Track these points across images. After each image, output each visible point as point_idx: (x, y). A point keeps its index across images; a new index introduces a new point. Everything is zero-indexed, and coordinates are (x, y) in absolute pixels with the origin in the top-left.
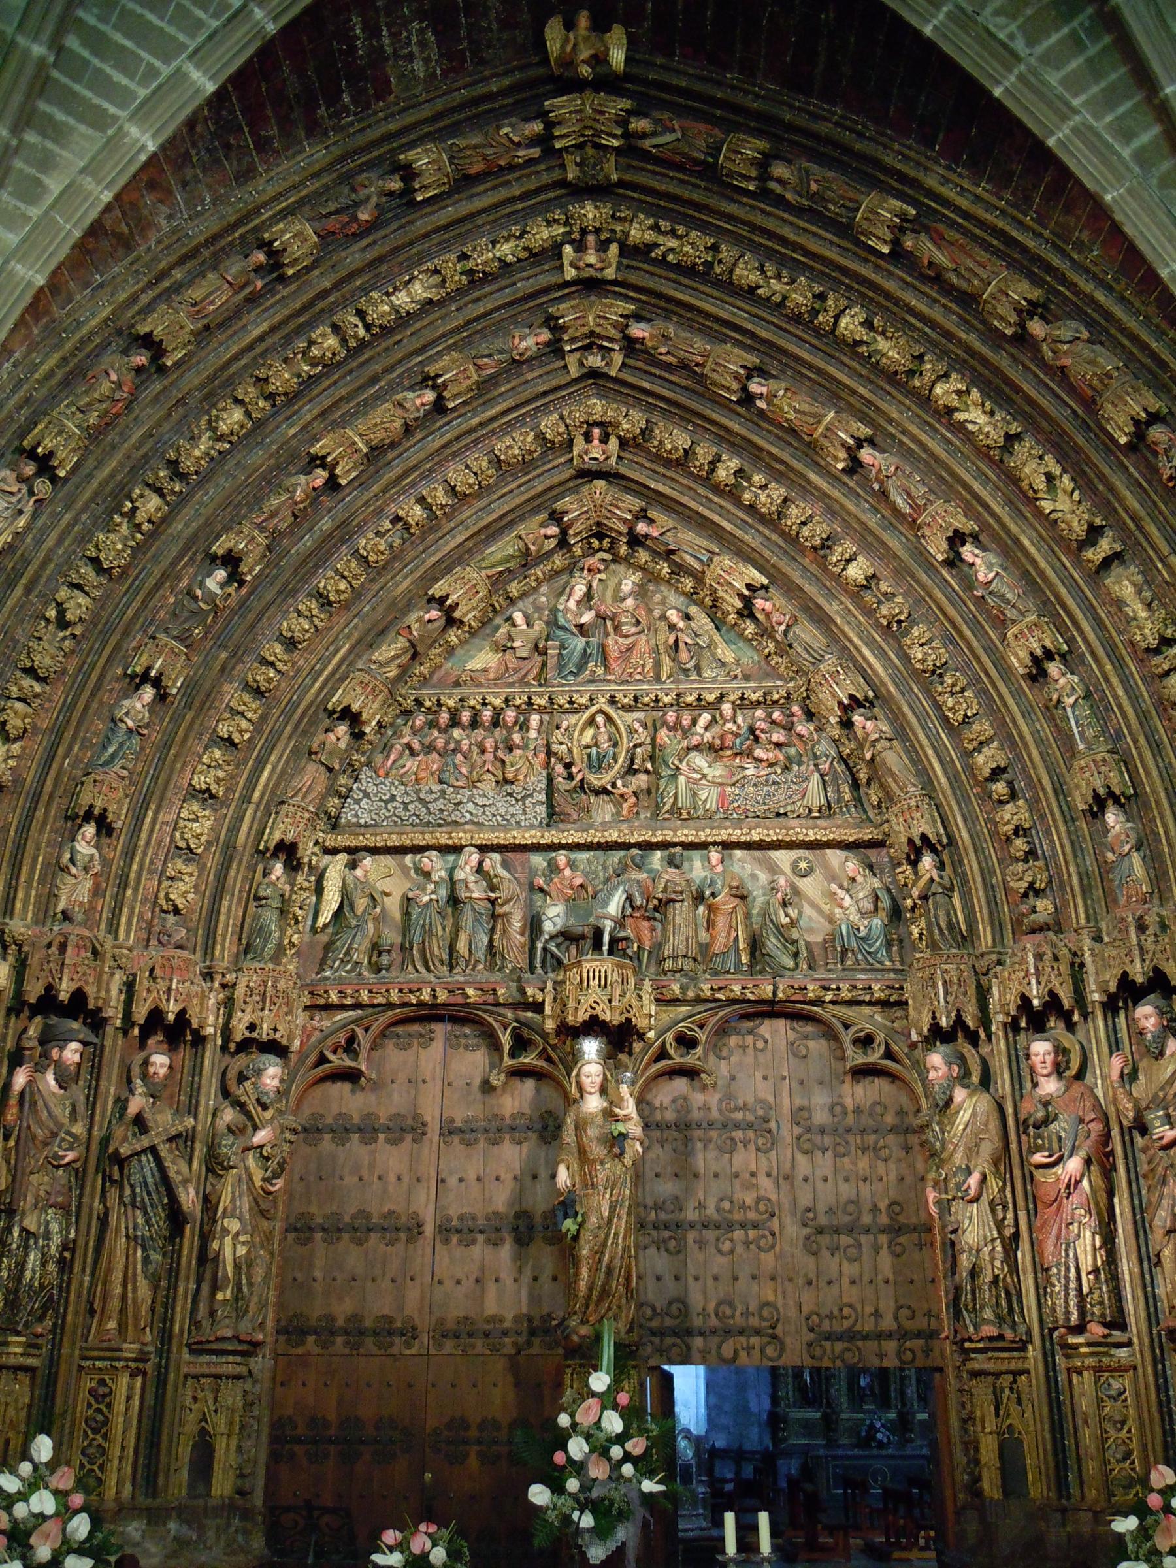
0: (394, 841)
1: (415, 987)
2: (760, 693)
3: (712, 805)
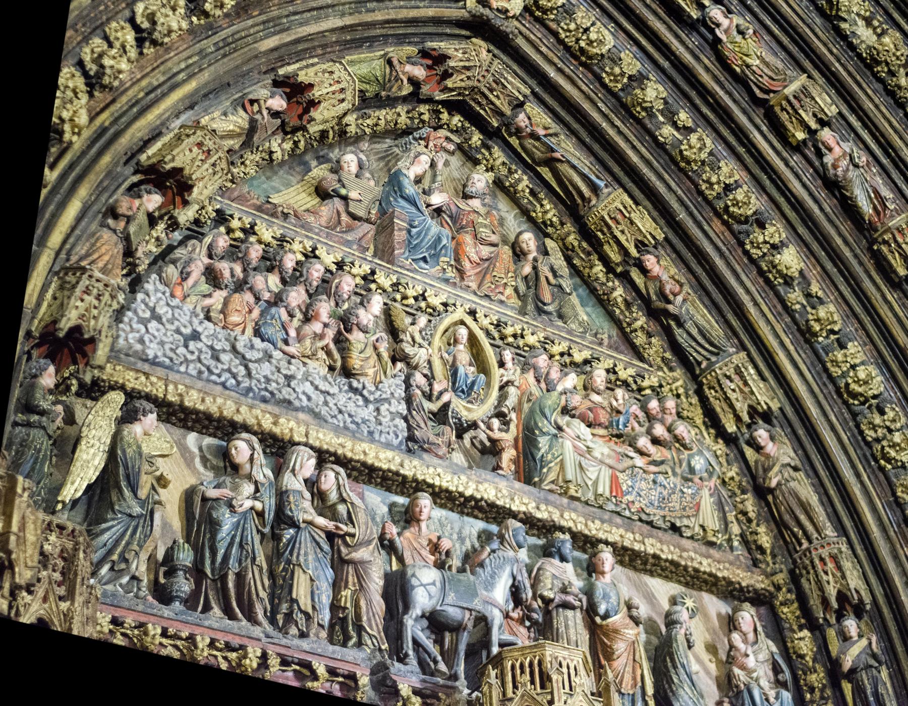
0: (192, 400)
1: (236, 641)
2: (631, 371)
3: (604, 488)
